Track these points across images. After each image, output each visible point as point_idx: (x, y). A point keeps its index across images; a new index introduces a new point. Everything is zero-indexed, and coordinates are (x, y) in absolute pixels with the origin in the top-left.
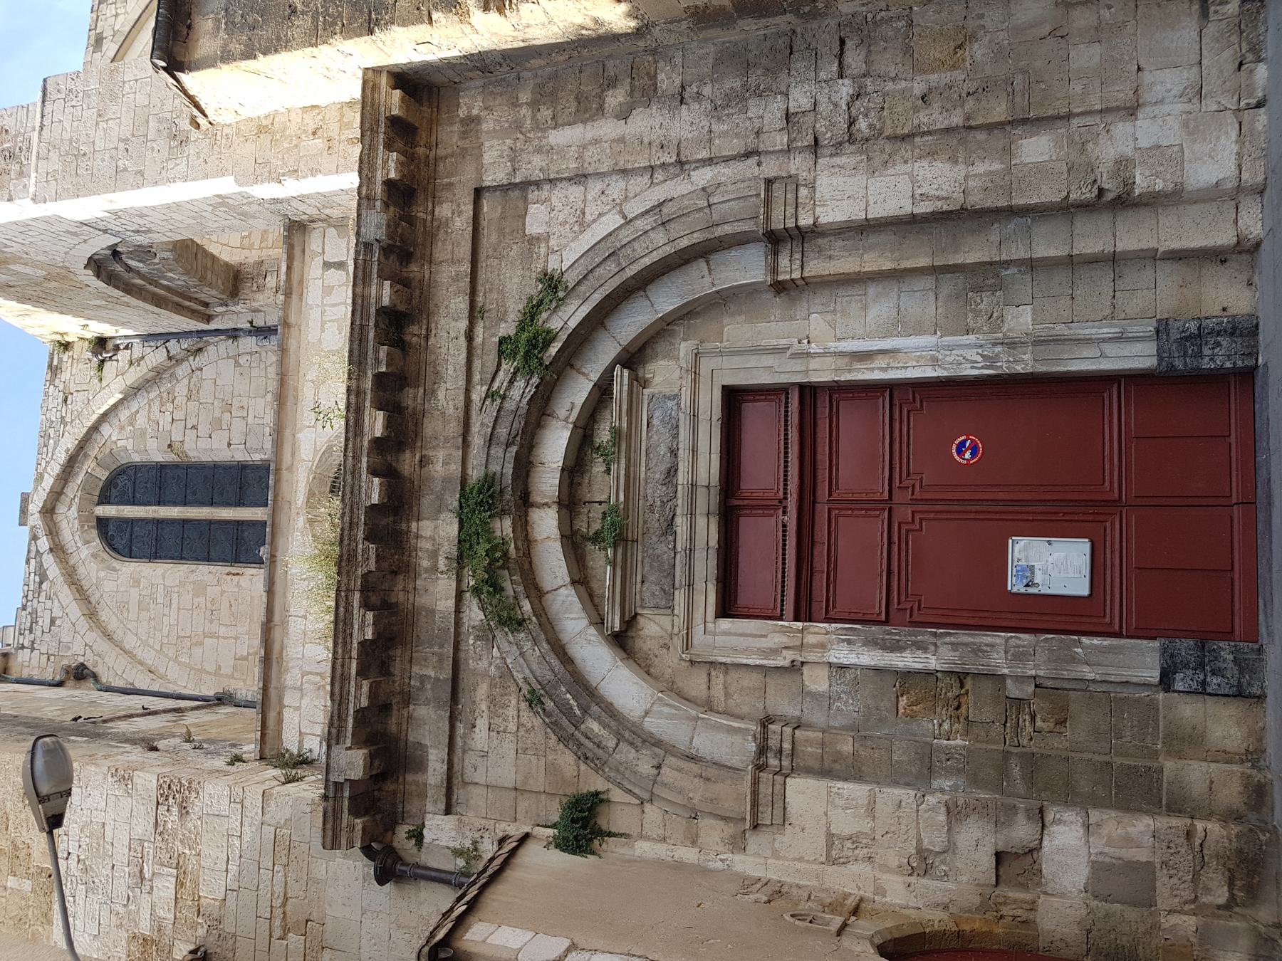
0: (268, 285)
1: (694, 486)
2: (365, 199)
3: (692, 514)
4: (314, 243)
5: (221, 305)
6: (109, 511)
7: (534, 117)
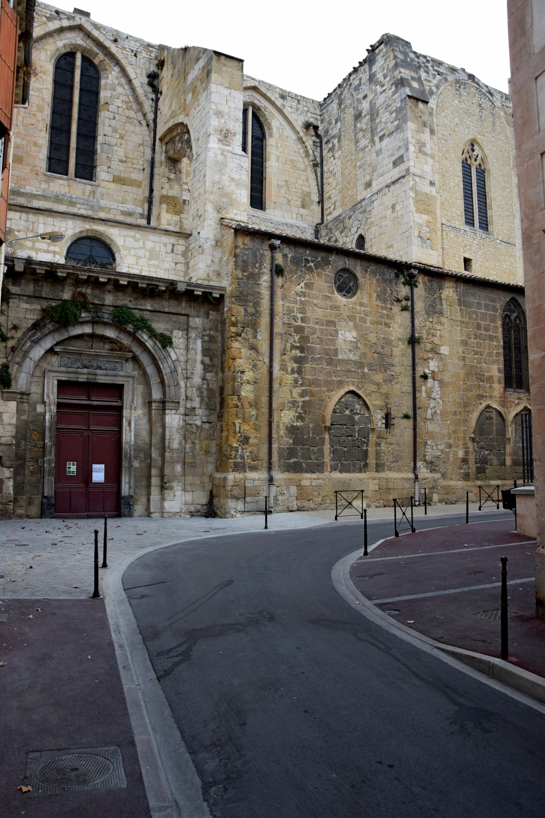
0: (171, 174)
1: (96, 375)
2: (189, 284)
3: (88, 374)
4: (182, 242)
5: (166, 150)
6: (78, 62)
7: (205, 335)
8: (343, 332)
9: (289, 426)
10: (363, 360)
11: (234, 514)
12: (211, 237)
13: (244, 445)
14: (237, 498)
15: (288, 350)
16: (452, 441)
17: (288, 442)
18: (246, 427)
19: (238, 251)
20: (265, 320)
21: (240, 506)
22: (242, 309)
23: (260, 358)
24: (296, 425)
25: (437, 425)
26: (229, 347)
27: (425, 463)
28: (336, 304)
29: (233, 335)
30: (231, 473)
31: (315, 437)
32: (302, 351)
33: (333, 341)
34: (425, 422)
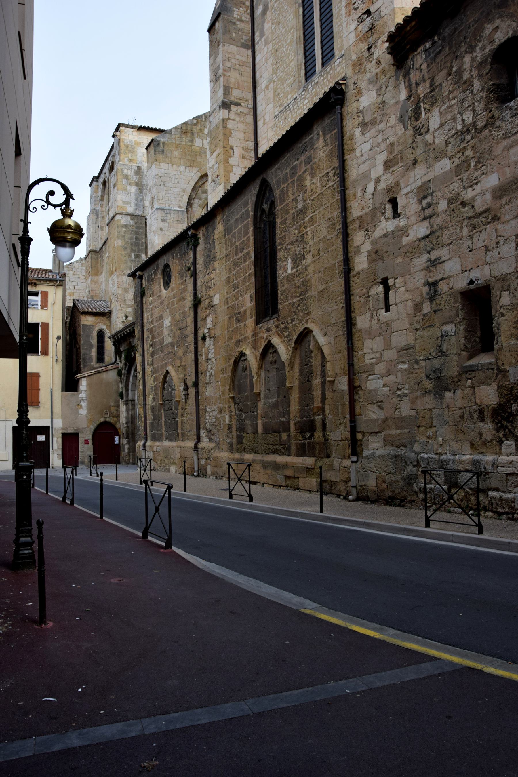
16: (221, 405)
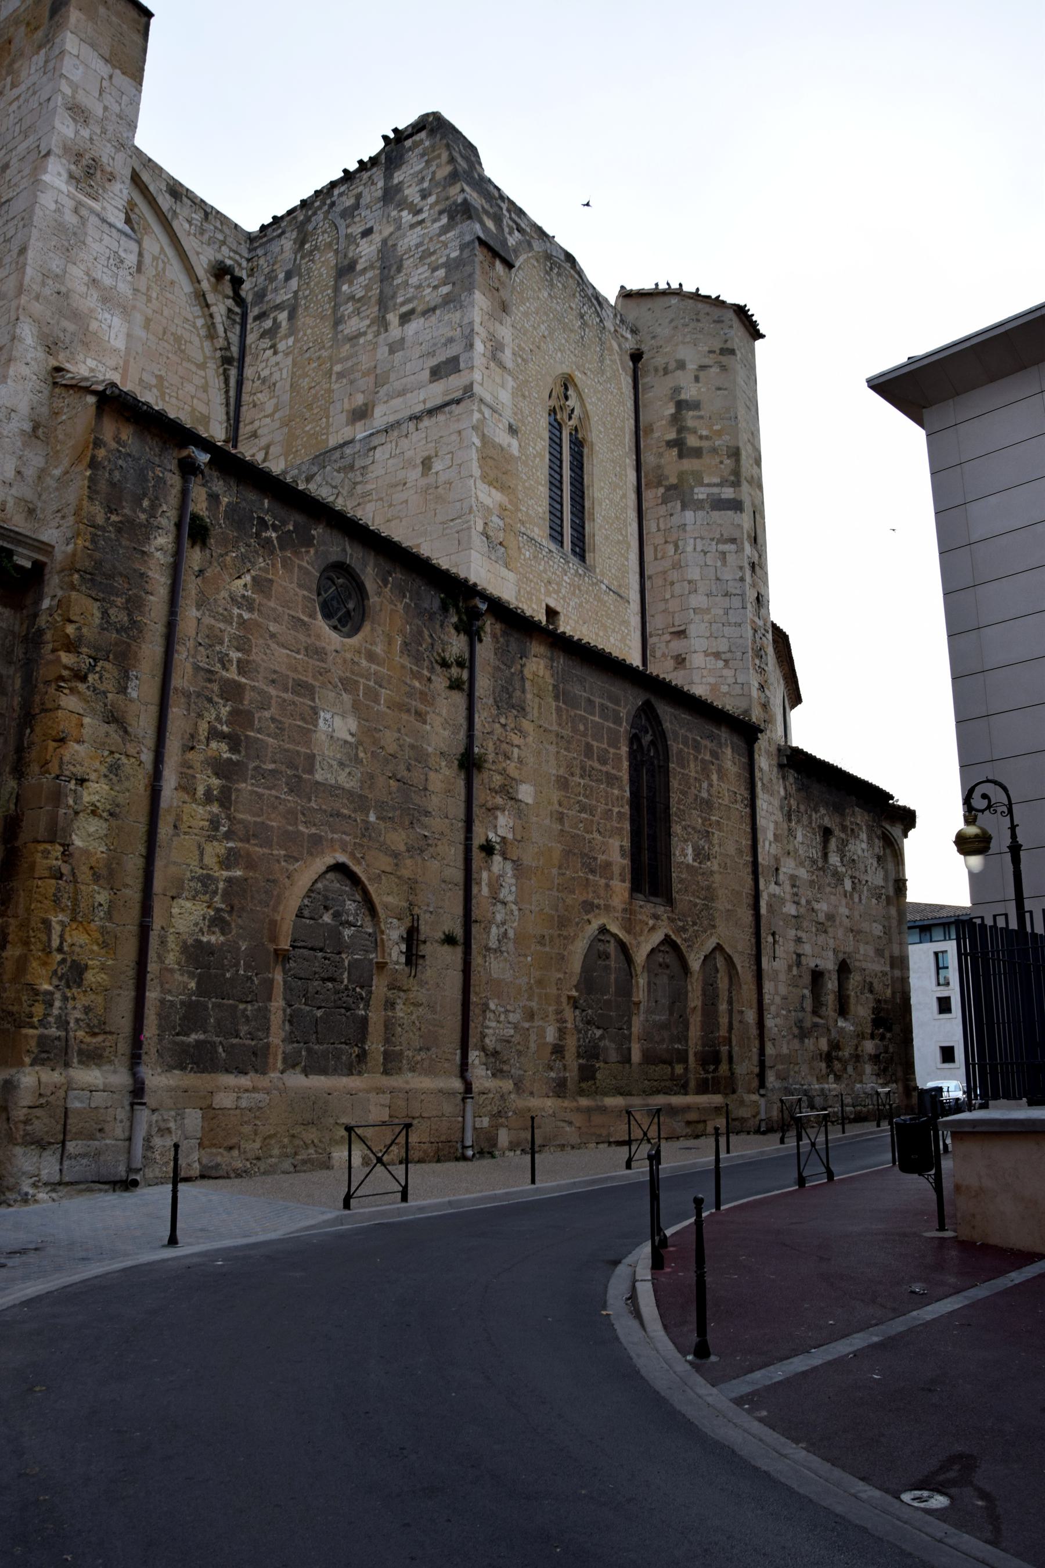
8: (328, 716)
9: (190, 941)
10: (366, 792)
11: (31, 1191)
12: (23, 407)
13: (69, 987)
14: (42, 1145)
15: (202, 738)
16: (534, 1004)
17: (185, 987)
18: (78, 937)
19: (101, 453)
20: (151, 650)
21: (49, 1166)
22: (95, 608)
23: (132, 751)
24: (209, 942)
25: (508, 966)
26: (49, 706)
27: (482, 1054)
28: (317, 643)
29: (65, 673)
30: (28, 1069)
31: (250, 978)
32: (234, 748)
33: (306, 734)
34: (485, 956)
